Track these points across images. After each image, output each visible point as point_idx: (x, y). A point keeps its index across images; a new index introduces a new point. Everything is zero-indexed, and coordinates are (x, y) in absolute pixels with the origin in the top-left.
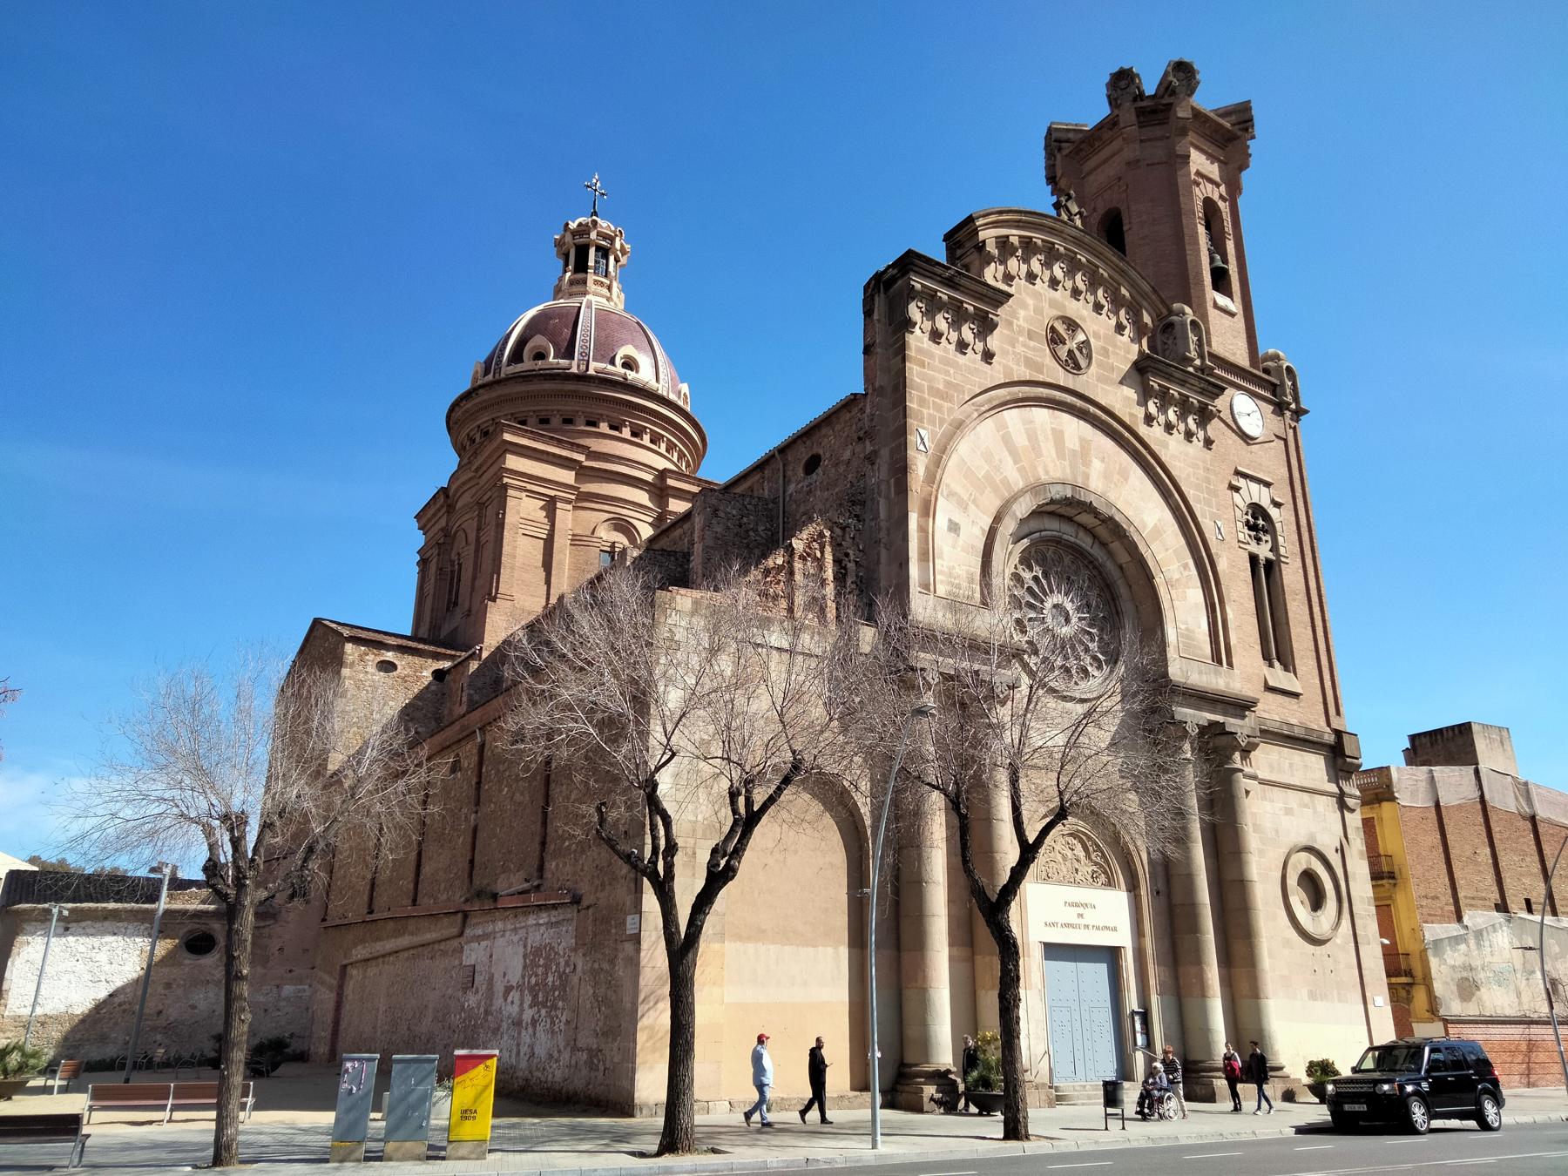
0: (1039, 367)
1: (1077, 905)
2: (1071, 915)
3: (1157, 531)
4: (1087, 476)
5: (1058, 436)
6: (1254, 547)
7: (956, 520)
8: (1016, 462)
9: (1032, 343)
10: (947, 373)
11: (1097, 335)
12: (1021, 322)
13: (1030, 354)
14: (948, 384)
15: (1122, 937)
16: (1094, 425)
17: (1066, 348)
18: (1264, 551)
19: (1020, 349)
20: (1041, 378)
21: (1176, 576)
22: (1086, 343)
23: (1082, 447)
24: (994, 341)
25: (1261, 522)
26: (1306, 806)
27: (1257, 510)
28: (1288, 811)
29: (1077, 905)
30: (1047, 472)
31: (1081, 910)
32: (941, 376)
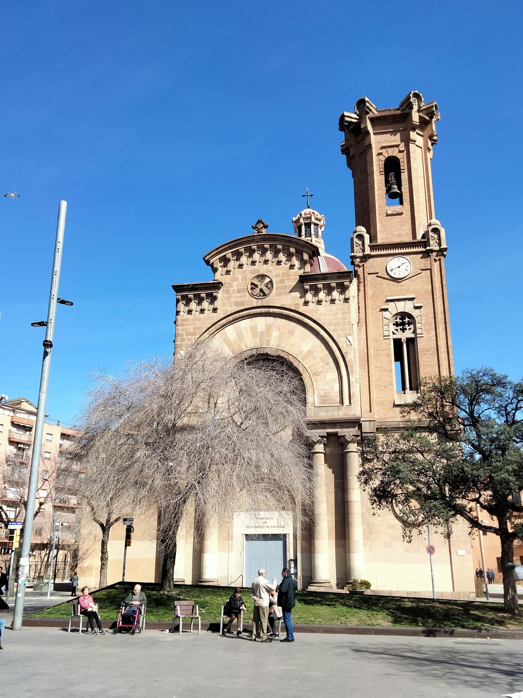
0: (242, 304)
3: (310, 353)
4: (268, 341)
5: (254, 329)
8: (229, 347)
10: (195, 324)
11: (277, 276)
12: (234, 288)
13: (238, 300)
15: (289, 530)
16: (275, 317)
17: (259, 288)
18: (404, 336)
19: (233, 300)
20: (243, 308)
22: (271, 282)
23: (267, 329)
24: (217, 304)
25: (407, 320)
27: (403, 315)
30: (246, 346)
32: (191, 327)
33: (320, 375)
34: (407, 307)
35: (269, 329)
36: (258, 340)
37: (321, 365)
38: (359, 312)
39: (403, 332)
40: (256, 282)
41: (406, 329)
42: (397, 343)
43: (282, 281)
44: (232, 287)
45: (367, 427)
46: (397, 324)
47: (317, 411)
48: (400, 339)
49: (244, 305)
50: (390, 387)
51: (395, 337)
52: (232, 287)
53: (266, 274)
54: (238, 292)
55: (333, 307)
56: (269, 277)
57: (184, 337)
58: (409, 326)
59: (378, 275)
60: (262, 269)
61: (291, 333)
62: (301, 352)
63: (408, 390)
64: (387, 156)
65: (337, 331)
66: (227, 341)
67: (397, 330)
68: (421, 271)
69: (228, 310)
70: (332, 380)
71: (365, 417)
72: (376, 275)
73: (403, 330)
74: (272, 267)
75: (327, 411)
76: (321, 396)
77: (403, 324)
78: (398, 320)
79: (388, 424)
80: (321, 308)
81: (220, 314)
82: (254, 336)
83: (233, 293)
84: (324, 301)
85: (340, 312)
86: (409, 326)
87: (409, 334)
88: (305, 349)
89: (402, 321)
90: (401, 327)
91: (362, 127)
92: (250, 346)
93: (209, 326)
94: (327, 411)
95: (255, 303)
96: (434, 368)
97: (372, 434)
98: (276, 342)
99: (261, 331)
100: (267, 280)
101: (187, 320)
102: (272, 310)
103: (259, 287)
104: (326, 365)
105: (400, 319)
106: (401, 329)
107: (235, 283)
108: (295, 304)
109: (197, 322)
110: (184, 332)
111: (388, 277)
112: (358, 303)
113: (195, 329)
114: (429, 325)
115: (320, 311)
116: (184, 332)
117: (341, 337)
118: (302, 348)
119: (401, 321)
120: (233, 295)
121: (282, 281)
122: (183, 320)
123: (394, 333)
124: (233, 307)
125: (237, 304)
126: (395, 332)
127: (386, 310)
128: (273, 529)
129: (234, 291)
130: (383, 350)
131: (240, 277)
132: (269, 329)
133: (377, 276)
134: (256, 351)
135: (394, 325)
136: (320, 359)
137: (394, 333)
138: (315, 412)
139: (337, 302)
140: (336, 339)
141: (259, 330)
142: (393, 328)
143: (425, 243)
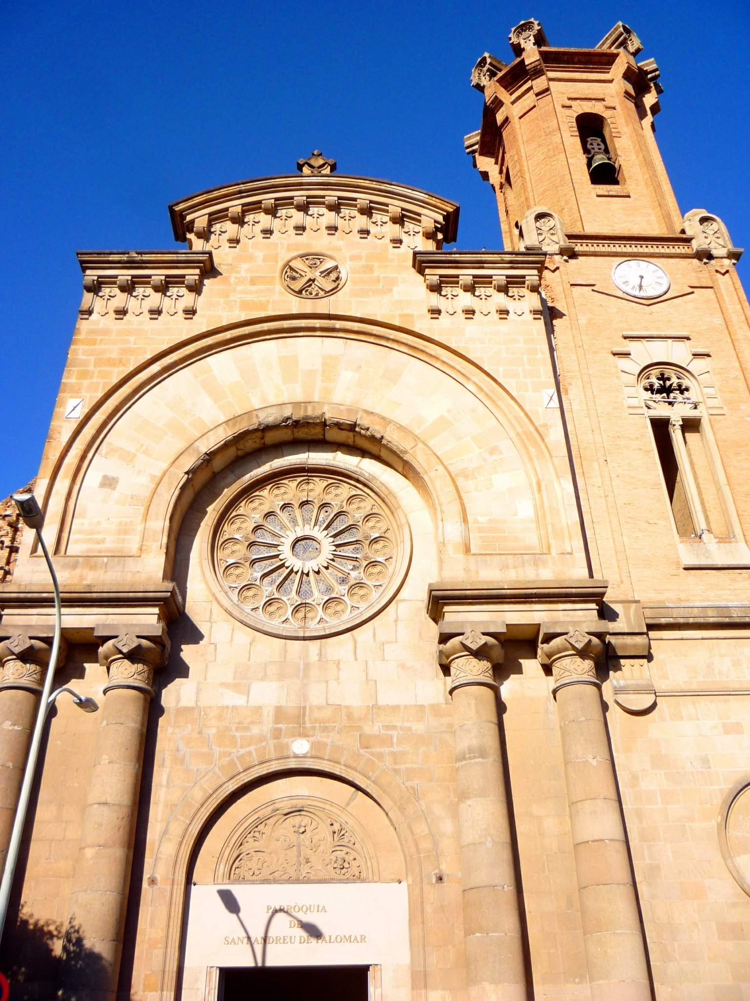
3: (442, 423)
5: (289, 365)
6: (661, 410)
7: (111, 474)
9: (255, 288)
11: (353, 258)
12: (243, 274)
13: (249, 297)
14: (124, 351)
18: (676, 413)
19: (235, 297)
34: (678, 353)
35: (330, 367)
40: (297, 264)
43: (369, 269)
44: (238, 272)
46: (650, 389)
49: (265, 309)
50: (662, 522)
52: (238, 272)
53: (328, 253)
54: (253, 281)
55: (504, 327)
56: (331, 258)
57: (91, 368)
59: (595, 288)
60: (319, 242)
64: (581, 112)
68: (691, 290)
75: (505, 567)
80: (471, 327)
81: (200, 325)
91: (526, 63)
92: (273, 401)
93: (165, 347)
94: (505, 567)
95: (296, 305)
101: (106, 332)
102: (338, 324)
107: (245, 266)
108: (401, 316)
109: (132, 339)
110: (92, 358)
111: (620, 294)
113: (124, 351)
116: (92, 358)
120: (239, 288)
122: (92, 332)
125: (245, 305)
126: (651, 403)
129: (240, 281)
131: (260, 255)
132: (330, 367)
134: (294, 408)
135: (646, 389)
138: (467, 570)
140: (514, 394)
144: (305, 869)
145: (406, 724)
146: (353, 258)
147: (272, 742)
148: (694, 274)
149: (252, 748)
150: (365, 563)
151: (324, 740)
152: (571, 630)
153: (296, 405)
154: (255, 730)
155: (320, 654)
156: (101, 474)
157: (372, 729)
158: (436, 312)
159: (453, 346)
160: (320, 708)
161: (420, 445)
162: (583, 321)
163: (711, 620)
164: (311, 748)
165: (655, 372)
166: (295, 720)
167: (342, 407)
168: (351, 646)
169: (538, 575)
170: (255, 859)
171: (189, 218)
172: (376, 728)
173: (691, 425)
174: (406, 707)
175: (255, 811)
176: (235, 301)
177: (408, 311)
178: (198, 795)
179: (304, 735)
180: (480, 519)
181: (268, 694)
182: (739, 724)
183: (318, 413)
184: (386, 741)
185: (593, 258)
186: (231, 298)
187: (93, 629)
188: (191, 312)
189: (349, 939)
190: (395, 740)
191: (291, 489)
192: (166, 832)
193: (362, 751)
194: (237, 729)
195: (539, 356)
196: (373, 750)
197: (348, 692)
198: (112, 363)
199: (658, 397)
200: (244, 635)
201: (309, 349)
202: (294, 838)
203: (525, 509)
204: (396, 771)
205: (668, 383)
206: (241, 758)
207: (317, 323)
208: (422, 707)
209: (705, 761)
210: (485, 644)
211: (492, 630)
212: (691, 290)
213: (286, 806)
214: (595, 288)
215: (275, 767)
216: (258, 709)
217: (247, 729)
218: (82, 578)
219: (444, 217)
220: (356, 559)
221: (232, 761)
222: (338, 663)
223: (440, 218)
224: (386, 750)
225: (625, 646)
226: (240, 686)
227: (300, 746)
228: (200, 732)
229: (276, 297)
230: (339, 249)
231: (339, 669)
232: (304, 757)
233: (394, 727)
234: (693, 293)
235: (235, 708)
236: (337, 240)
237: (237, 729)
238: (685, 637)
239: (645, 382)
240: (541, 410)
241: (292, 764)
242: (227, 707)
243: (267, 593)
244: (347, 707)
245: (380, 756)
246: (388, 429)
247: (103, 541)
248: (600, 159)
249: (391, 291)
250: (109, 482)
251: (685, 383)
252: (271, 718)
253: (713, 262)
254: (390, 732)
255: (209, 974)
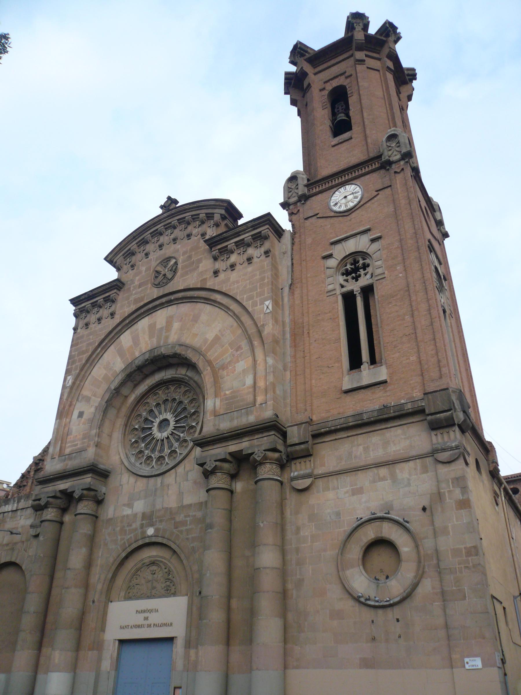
0: (142, 299)
1: (144, 611)
2: (139, 619)
3: (217, 339)
4: (167, 338)
18: (355, 286)
19: (132, 298)
20: (142, 304)
21: (229, 359)
23: (167, 322)
26: (383, 479)
28: (358, 491)
29: (144, 611)
31: (146, 615)
33: (227, 368)
34: (361, 243)
36: (155, 340)
37: (230, 353)
38: (292, 271)
39: (357, 280)
40: (159, 269)
41: (360, 276)
42: (349, 299)
43: (190, 257)
45: (295, 435)
46: (347, 273)
47: (217, 423)
48: (352, 292)
51: (344, 290)
53: (173, 255)
54: (140, 286)
55: (250, 269)
56: (174, 258)
58: (365, 270)
59: (318, 216)
60: (168, 251)
61: (196, 319)
62: (206, 340)
63: (365, 366)
65: (251, 298)
66: (121, 353)
67: (347, 281)
68: (377, 193)
69: (125, 312)
70: (244, 371)
71: (286, 417)
72: (315, 217)
73: (356, 279)
74: (179, 246)
75: (232, 420)
76: (227, 399)
77: (356, 270)
78: (349, 267)
79: (330, 424)
80: (234, 275)
81: (118, 319)
82: (151, 336)
83: (133, 290)
84: (238, 265)
85: (258, 273)
86: (365, 270)
87: (364, 281)
88: (210, 336)
89: (355, 266)
90: (354, 275)
95: (156, 293)
96: (404, 319)
97: (302, 446)
98: (176, 337)
99: (160, 326)
100: (173, 261)
102: (172, 297)
103: (163, 273)
104: (237, 351)
105: (352, 264)
106: (353, 278)
107: (137, 278)
111: (333, 214)
112: (292, 259)
114: (393, 259)
115: (231, 280)
117: (257, 306)
118: (207, 336)
119: (353, 267)
121: (190, 257)
123: (342, 286)
124: (132, 307)
125: (136, 301)
127: (330, 256)
128: (156, 629)
130: (326, 313)
131: (144, 269)
133: (318, 218)
135: (343, 274)
136: (230, 344)
137: (342, 286)
138: (214, 425)
139: (255, 260)
140: (250, 309)
141: (158, 326)
142: (341, 279)
143: (380, 157)
144: (154, 592)
145: (194, 513)
146: (184, 253)
147: (140, 531)
148: (380, 181)
149: (132, 535)
150: (187, 428)
151: (160, 526)
152: (256, 450)
153: (151, 351)
154: (134, 526)
155: (161, 483)
156: (78, 411)
157: (180, 518)
158: (216, 273)
159: (224, 290)
160: (159, 510)
161: (202, 357)
162: (309, 241)
163: (351, 424)
164: (155, 531)
165: (350, 260)
166: (149, 518)
167: (169, 346)
168: (173, 476)
169: (247, 420)
170: (136, 588)
171: (115, 261)
172: (181, 517)
173: (368, 291)
174: (195, 504)
175: (135, 565)
176: (132, 301)
177: (205, 277)
178: (111, 560)
179: (152, 525)
180: (227, 392)
181: (139, 506)
182: (362, 488)
183: (159, 353)
184: (184, 523)
185: (320, 195)
186: (130, 299)
187: (67, 489)
188: (112, 314)
189: (165, 625)
190: (188, 523)
191: (162, 395)
192: (99, 579)
193: (174, 530)
194: (128, 526)
195: (266, 281)
196: (179, 529)
197: (171, 501)
198: (83, 353)
199: (349, 277)
200: (132, 479)
201: (160, 317)
202: (150, 577)
203: (249, 381)
204: (187, 539)
205: (357, 265)
206: (128, 540)
207: (164, 300)
208: (202, 503)
209: (338, 514)
210: (216, 466)
211: (219, 458)
212: (377, 193)
213: (147, 561)
214: (318, 216)
215: (140, 543)
216: (137, 514)
217: (131, 525)
218: (67, 465)
219: (226, 211)
220: (184, 427)
221: (125, 542)
222: (168, 486)
223: (223, 212)
224: (184, 528)
225: (296, 451)
226: (130, 505)
227: (150, 531)
228: (114, 530)
229: (148, 291)
230: (177, 251)
231: (168, 489)
232: (152, 536)
233: (189, 516)
234: (378, 194)
235: (128, 516)
236: (178, 246)
237: (128, 526)
238: (337, 437)
239: (343, 270)
240: (262, 316)
241: (147, 541)
242: (124, 516)
243: (146, 454)
244: (171, 508)
245: (181, 532)
246: (188, 352)
247: (77, 445)
248: (342, 116)
249: (198, 267)
250: (81, 414)
251: (367, 261)
252: (140, 518)
253: (394, 166)
254: (187, 519)
255: (114, 643)
